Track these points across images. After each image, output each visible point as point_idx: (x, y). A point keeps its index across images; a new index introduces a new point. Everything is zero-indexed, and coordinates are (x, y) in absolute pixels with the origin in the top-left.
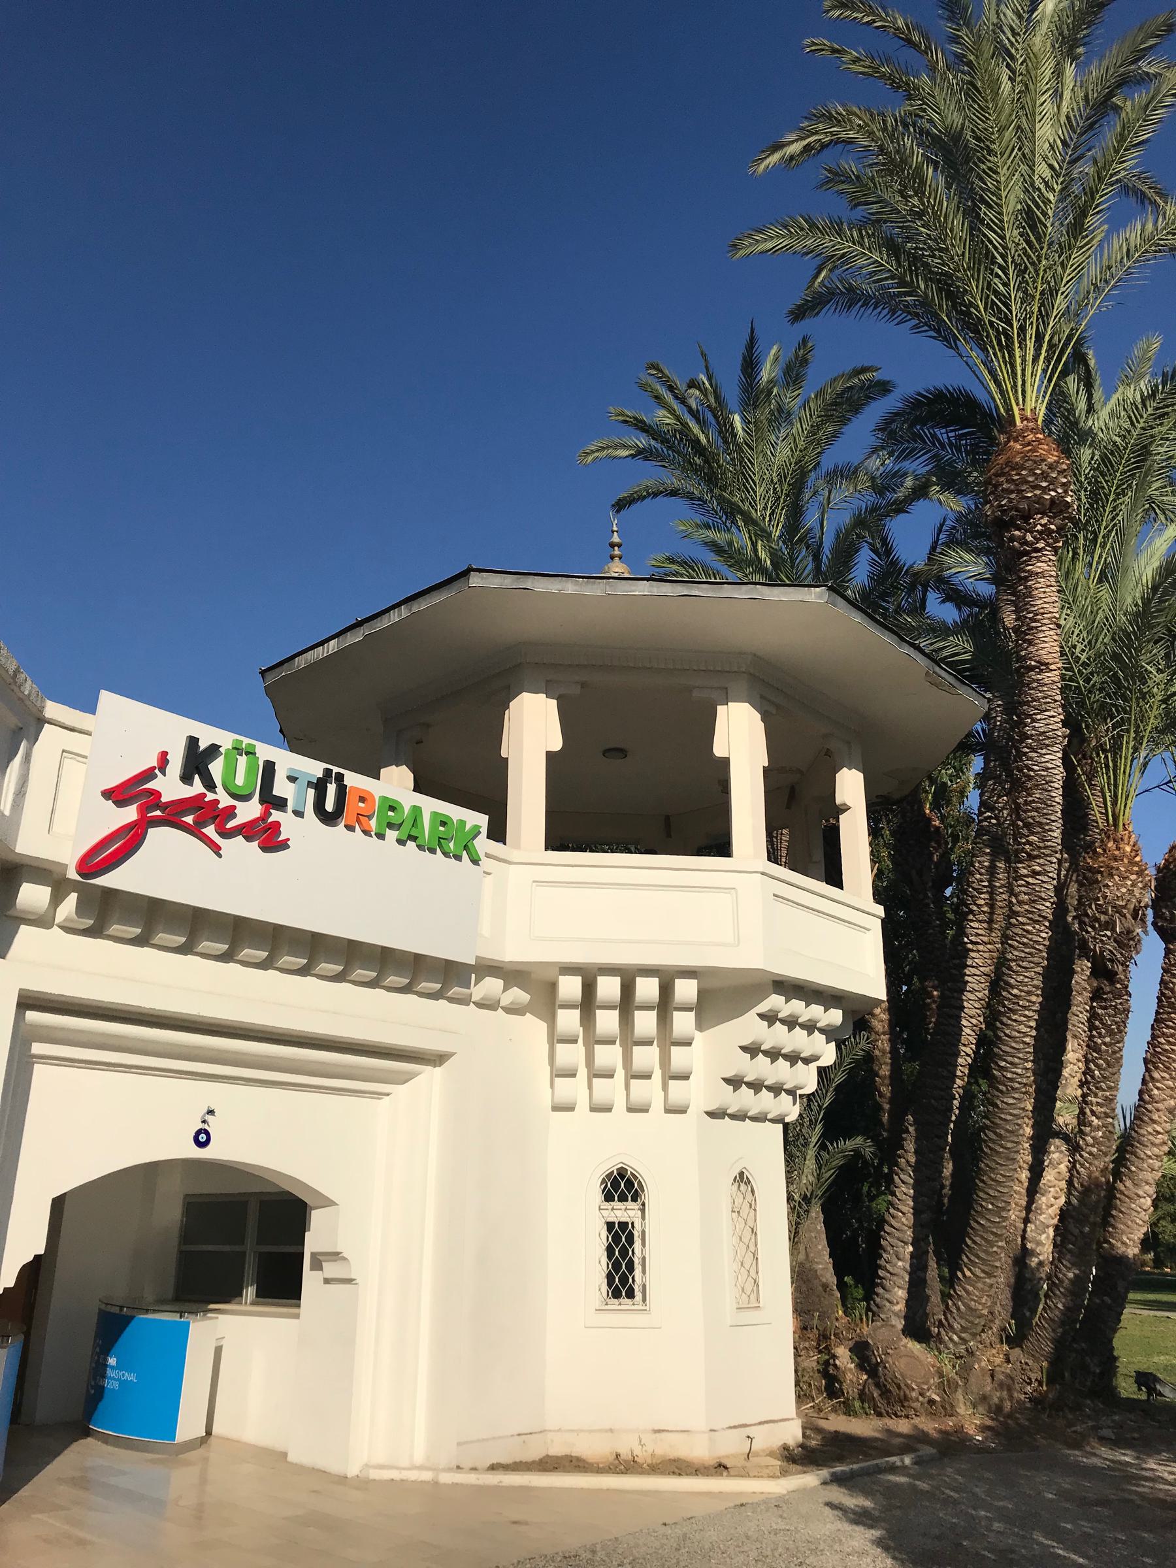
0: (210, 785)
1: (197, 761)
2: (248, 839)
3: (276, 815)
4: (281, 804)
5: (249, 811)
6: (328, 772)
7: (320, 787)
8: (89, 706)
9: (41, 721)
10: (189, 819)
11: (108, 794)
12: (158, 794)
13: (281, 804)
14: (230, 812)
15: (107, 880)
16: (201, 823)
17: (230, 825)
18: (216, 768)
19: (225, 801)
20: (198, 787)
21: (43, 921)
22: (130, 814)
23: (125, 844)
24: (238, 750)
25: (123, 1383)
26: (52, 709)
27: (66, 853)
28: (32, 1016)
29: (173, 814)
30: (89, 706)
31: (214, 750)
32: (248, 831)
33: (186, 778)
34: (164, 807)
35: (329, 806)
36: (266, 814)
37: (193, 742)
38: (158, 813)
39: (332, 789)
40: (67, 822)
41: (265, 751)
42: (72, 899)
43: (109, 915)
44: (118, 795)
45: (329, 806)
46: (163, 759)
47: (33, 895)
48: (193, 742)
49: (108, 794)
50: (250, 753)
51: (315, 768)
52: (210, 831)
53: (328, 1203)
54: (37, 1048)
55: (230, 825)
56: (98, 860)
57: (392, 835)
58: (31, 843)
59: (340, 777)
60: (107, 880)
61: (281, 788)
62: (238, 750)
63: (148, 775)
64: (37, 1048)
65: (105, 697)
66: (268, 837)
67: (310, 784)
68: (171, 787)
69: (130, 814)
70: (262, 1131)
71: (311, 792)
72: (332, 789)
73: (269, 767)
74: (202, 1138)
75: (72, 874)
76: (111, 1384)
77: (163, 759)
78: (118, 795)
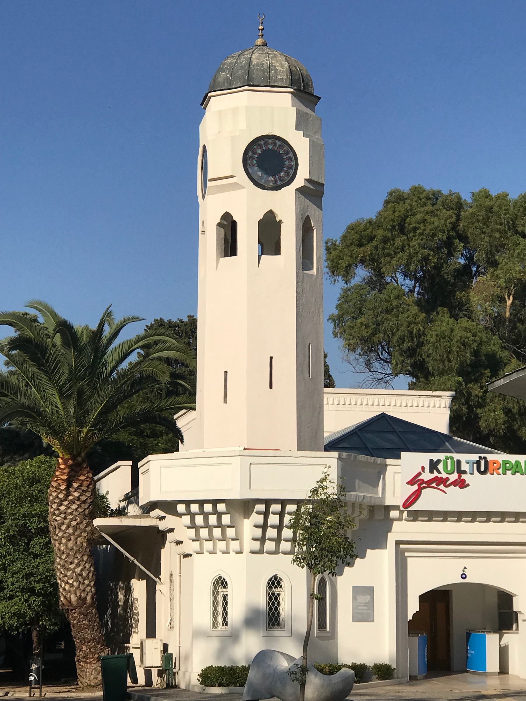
0: (439, 472)
1: (434, 465)
2: (455, 486)
3: (464, 476)
4: (465, 472)
5: (454, 477)
6: (480, 457)
7: (478, 463)
8: (399, 457)
9: (386, 466)
10: (434, 485)
11: (408, 483)
12: (422, 480)
13: (465, 472)
14: (447, 479)
15: (413, 508)
16: (438, 485)
17: (448, 483)
18: (440, 467)
19: (444, 475)
20: (436, 474)
21: (400, 519)
22: (416, 487)
23: (416, 496)
24: (447, 458)
25: (472, 654)
26: (389, 461)
27: (400, 502)
28: (402, 546)
29: (429, 484)
30: (399, 457)
31: (439, 461)
32: (454, 483)
33: (431, 472)
34: (426, 483)
35: (483, 469)
36: (460, 477)
37: (431, 461)
38: (424, 485)
39: (483, 462)
40: (398, 493)
41: (457, 456)
42: (405, 513)
43: (415, 516)
44: (411, 483)
45: (483, 469)
46: (423, 468)
47: (394, 514)
48: (431, 461)
49: (408, 483)
50: (452, 458)
51: (475, 457)
52: (442, 487)
53: (516, 595)
54: (406, 554)
55: (448, 483)
56: (408, 503)
57: (509, 473)
58: (388, 502)
59: (485, 458)
60: (413, 508)
61: (465, 467)
62: (447, 458)
63: (419, 474)
64: (406, 554)
65: (403, 454)
66: (462, 484)
67: (473, 463)
68: (427, 476)
69: (416, 487)
70: (485, 572)
71: (475, 465)
72: (483, 462)
73: (459, 462)
74: (464, 576)
75: (402, 508)
76: (469, 655)
77: (423, 468)
78: (411, 483)
